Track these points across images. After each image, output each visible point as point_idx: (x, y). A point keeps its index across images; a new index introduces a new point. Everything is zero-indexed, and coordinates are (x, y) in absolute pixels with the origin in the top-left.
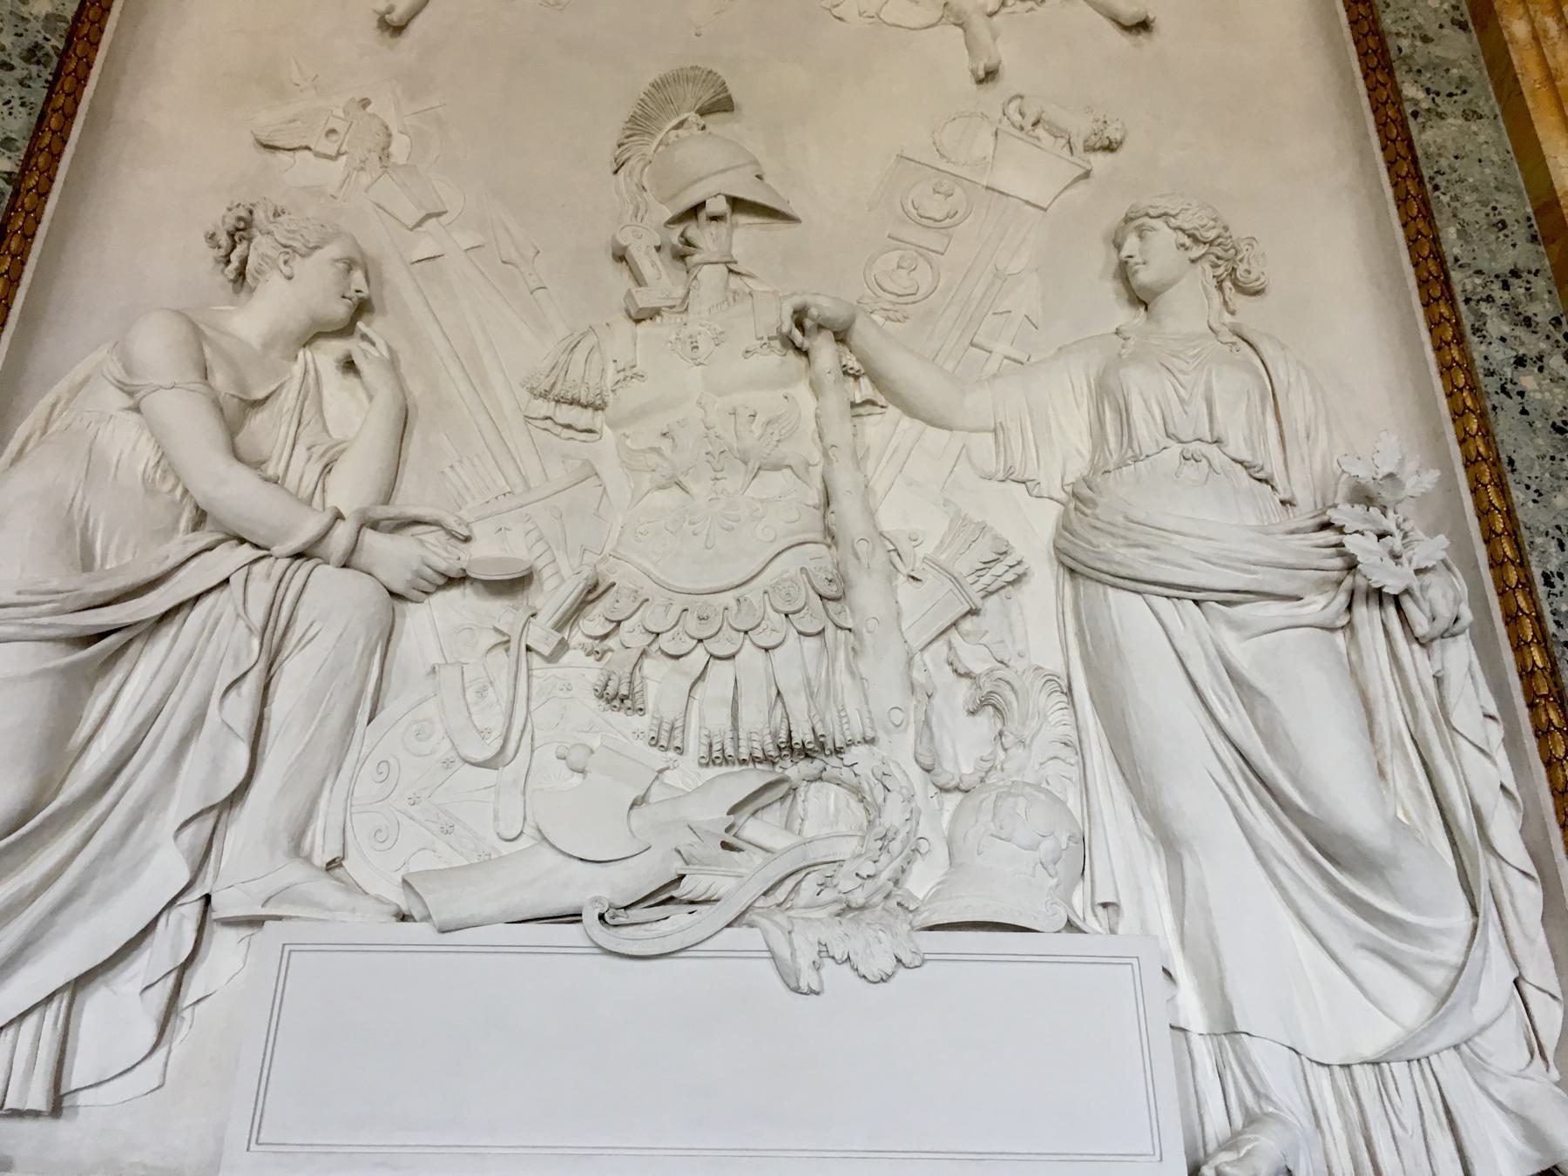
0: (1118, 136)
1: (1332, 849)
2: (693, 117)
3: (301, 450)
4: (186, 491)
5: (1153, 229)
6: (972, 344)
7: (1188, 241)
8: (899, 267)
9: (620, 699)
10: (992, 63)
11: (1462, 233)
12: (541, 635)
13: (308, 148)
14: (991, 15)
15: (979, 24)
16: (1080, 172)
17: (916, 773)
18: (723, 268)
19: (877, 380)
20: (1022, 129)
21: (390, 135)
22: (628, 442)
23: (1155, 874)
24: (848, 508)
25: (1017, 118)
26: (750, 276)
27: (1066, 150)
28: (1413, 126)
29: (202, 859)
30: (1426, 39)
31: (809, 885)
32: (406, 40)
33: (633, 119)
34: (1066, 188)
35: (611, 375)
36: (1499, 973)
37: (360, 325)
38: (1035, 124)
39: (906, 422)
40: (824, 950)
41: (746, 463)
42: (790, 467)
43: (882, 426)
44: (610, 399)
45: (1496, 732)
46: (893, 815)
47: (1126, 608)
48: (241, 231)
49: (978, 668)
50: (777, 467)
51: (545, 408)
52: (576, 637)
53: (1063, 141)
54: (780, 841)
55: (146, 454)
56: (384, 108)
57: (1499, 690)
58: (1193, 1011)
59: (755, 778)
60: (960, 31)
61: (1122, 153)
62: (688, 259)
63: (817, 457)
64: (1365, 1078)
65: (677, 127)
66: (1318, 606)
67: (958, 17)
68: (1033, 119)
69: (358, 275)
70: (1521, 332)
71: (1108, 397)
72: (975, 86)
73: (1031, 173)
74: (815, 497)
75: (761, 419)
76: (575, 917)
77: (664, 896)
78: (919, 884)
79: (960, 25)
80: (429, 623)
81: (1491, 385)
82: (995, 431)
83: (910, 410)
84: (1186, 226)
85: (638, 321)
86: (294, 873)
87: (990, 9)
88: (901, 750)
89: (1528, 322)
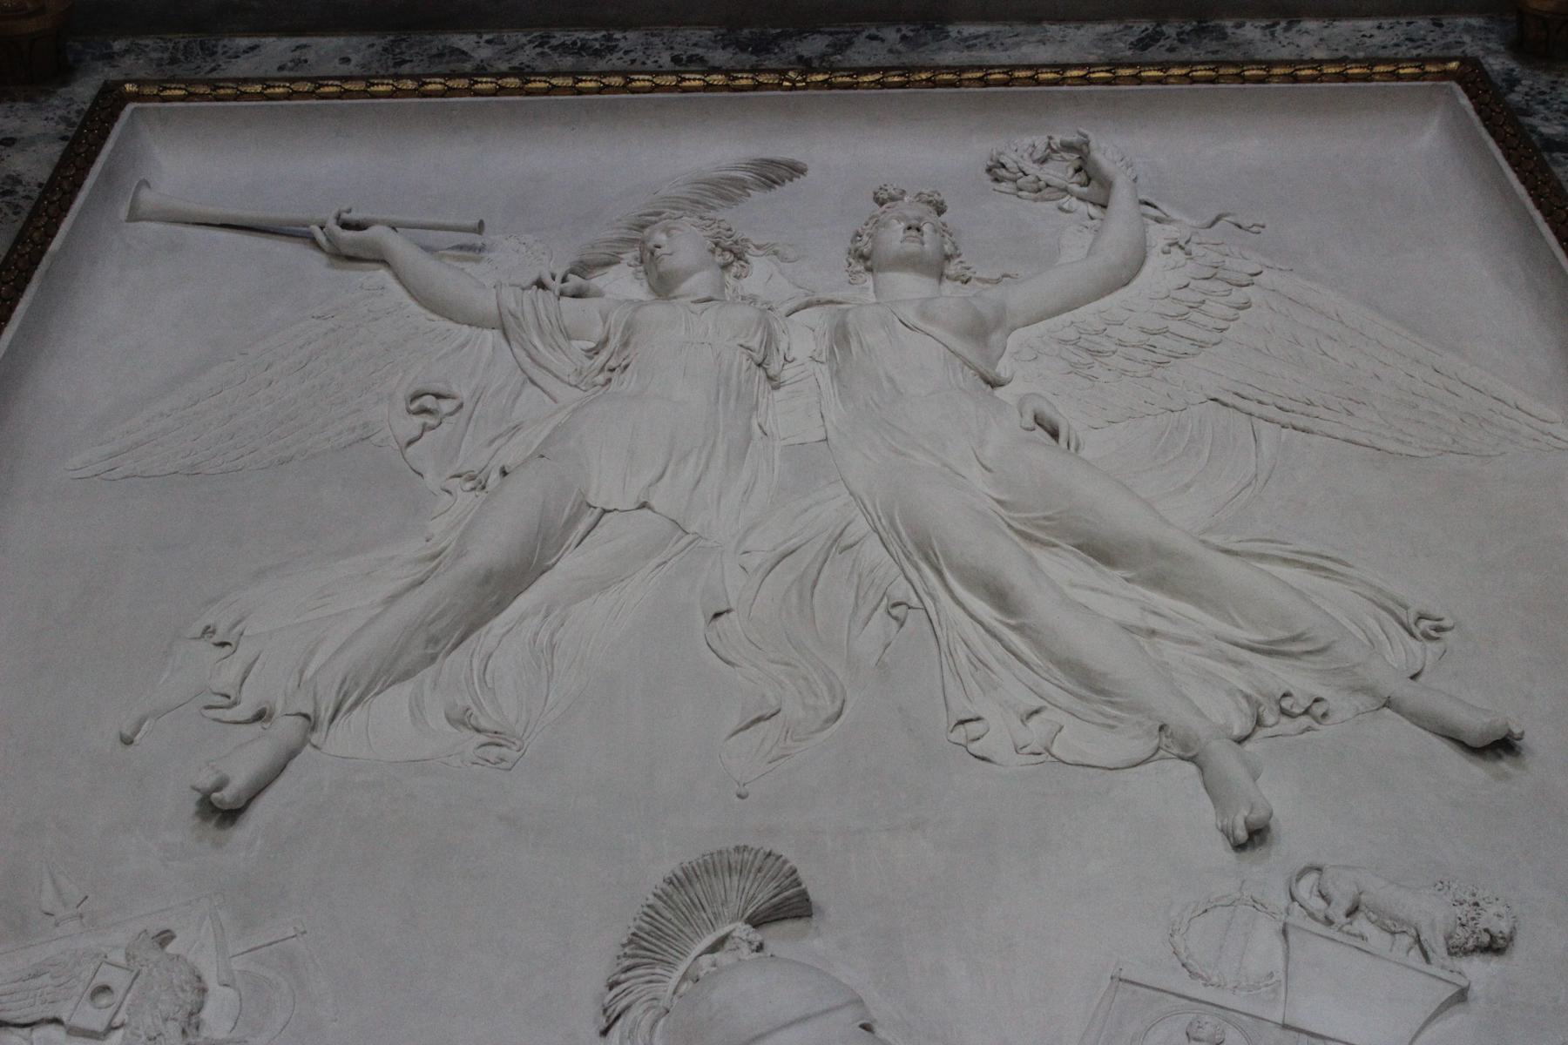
0: (1503, 926)
2: (741, 929)
10: (1258, 815)
13: (56, 1021)
14: (1241, 741)
15: (1226, 759)
16: (1451, 991)
20: (1329, 922)
21: (204, 991)
25: (1317, 904)
27: (1415, 953)
32: (242, 832)
33: (634, 939)
38: (1352, 912)
53: (1406, 940)
56: (198, 946)
60: (1191, 768)
65: (713, 949)
67: (1185, 746)
68: (1346, 905)
72: (1231, 856)
79: (1192, 760)
87: (1237, 731)
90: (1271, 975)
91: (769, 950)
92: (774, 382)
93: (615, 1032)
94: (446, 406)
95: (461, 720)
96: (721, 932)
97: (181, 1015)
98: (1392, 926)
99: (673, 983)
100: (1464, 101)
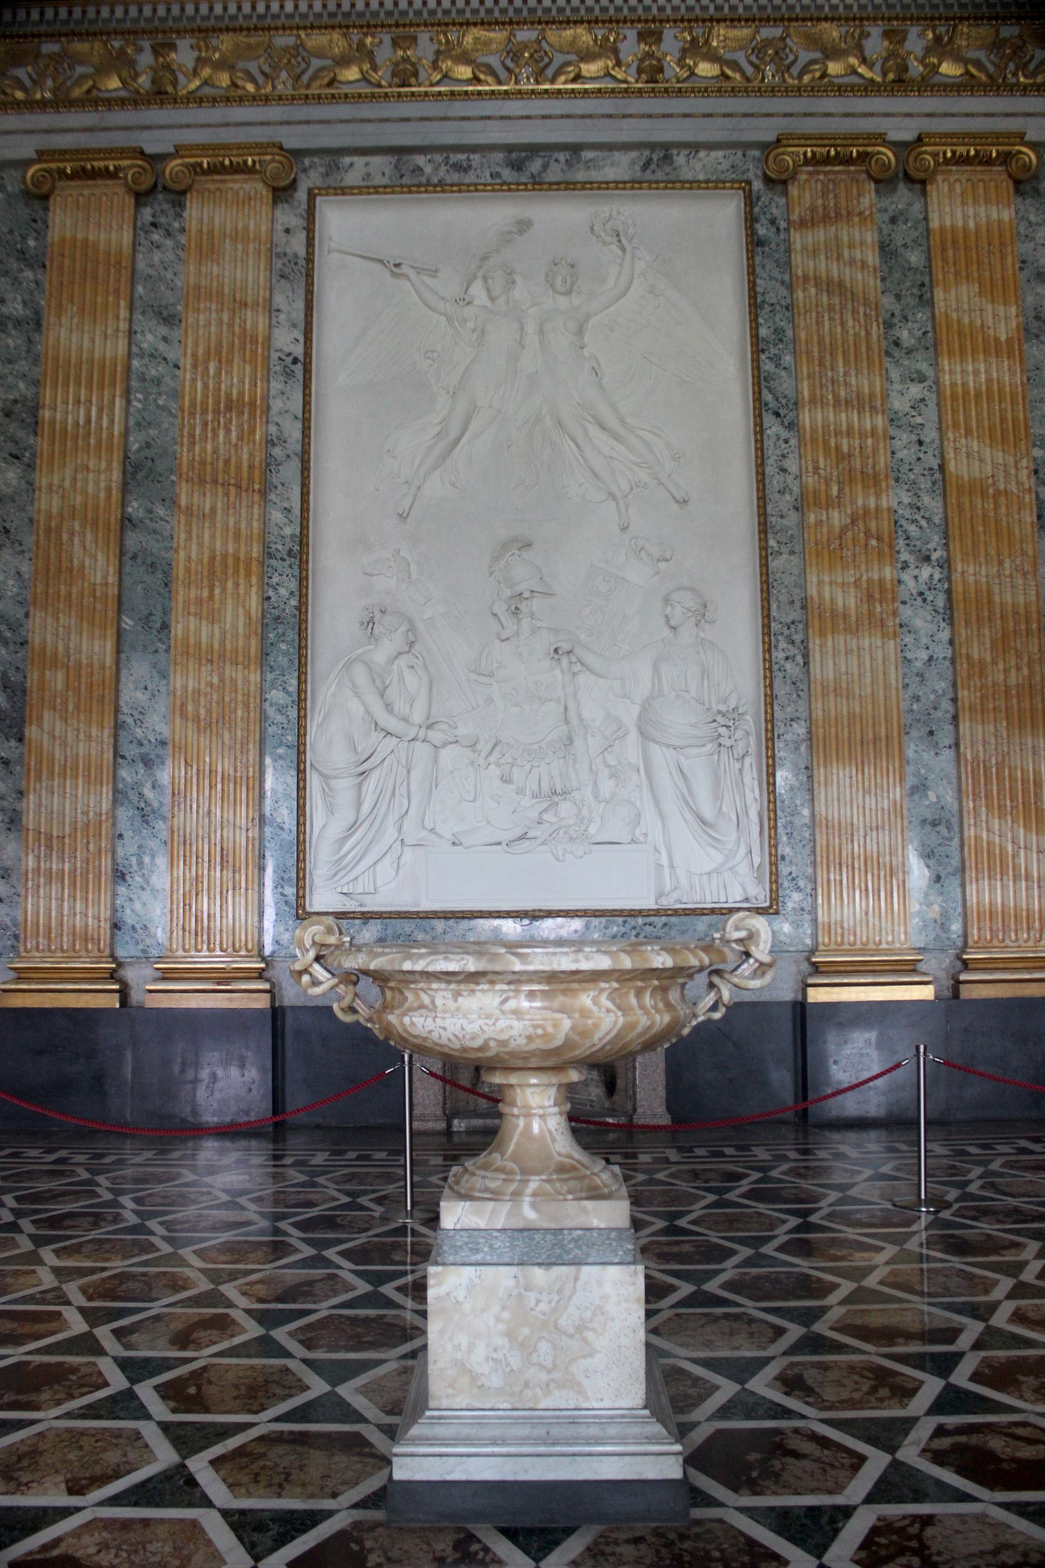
1: (703, 821)
9: (506, 780)
11: (778, 607)
12: (481, 761)
17: (591, 798)
19: (582, 664)
23: (659, 824)
24: (572, 715)
28: (770, 558)
29: (400, 830)
30: (782, 517)
31: (562, 832)
32: (409, 519)
35: (495, 665)
36: (743, 850)
39: (592, 677)
40: (565, 851)
43: (584, 679)
45: (756, 783)
46: (585, 812)
47: (655, 750)
48: (372, 621)
49: (612, 763)
51: (474, 676)
52: (492, 759)
54: (554, 820)
55: (362, 710)
57: (760, 771)
58: (664, 860)
59: (546, 805)
64: (706, 877)
66: (709, 747)
70: (790, 647)
71: (656, 669)
74: (562, 709)
76: (499, 843)
77: (523, 837)
78: (592, 829)
80: (447, 755)
81: (775, 667)
83: (593, 672)
86: (424, 834)
88: (588, 792)
89: (793, 642)
94: (435, 355)
95: (453, 485)
98: (649, 555)
100: (742, 205)
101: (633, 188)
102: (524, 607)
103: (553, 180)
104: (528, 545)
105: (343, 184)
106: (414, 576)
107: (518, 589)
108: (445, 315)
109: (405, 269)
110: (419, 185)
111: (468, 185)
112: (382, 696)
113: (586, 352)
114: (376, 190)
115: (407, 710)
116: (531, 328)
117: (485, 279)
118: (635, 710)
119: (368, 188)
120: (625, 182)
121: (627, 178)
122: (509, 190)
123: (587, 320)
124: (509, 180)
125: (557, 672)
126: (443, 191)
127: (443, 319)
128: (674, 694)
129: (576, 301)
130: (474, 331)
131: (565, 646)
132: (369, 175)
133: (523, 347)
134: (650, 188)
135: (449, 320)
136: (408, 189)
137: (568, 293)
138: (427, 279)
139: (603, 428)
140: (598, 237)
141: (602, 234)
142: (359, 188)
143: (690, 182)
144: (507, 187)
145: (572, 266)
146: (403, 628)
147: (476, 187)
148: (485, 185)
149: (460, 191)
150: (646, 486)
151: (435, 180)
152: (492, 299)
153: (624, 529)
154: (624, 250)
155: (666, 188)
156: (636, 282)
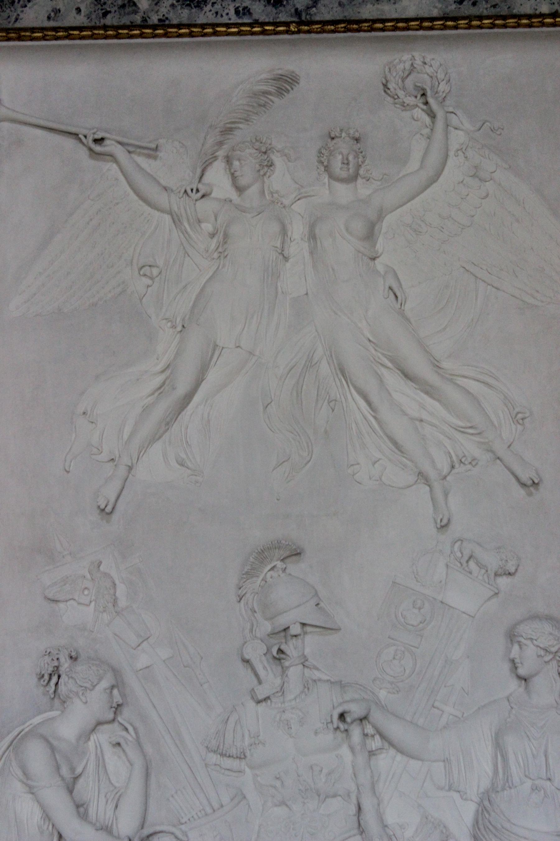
2: (279, 564)
3: (102, 796)
4: (53, 825)
5: (526, 645)
6: (433, 706)
7: (542, 653)
8: (394, 658)
13: (75, 600)
16: (492, 593)
18: (301, 666)
22: (259, 779)
24: (369, 817)
26: (317, 669)
32: (115, 517)
34: (485, 602)
35: (247, 741)
37: (119, 719)
39: (399, 757)
41: (319, 796)
42: (340, 795)
43: (386, 761)
44: (248, 754)
48: (56, 673)
50: (335, 796)
51: (214, 758)
55: (37, 814)
60: (428, 488)
61: (518, 574)
62: (282, 661)
63: (353, 788)
69: (115, 692)
71: (498, 745)
72: (435, 530)
73: (465, 596)
74: (353, 809)
75: (325, 771)
79: (429, 486)
82: (444, 761)
84: (541, 646)
85: (259, 702)
90: (441, 582)
91: (287, 571)
92: (286, 259)
93: (242, 601)
94: (155, 271)
95: (182, 464)
96: (272, 565)
97: (112, 600)
98: (480, 565)
99: (259, 582)
101: (445, 27)
102: (290, 648)
103: (328, 17)
104: (297, 554)
105: (18, 25)
106: (123, 602)
107: (282, 621)
108: (170, 213)
109: (110, 147)
110: (131, 26)
111: (203, 26)
112: (71, 791)
113: (379, 265)
114: (69, 33)
115: (110, 813)
116: (298, 230)
117: (228, 160)
118: (469, 811)
119: (55, 29)
120: (432, 19)
121: (435, 13)
122: (264, 32)
123: (381, 217)
124: (263, 18)
125: (345, 751)
126: (166, 35)
127: (167, 218)
128: (528, 784)
129: (363, 189)
130: (212, 235)
131: (356, 710)
132: (57, 11)
133: (286, 259)
134: (470, 27)
135: (176, 220)
136: (116, 32)
137: (353, 178)
138: (140, 160)
139: (407, 376)
140: (395, 97)
141: (401, 93)
142: (42, 29)
143: (529, 17)
144: (261, 28)
145: (357, 140)
146: (105, 684)
147: (213, 29)
148: (228, 25)
149: (191, 35)
150: (474, 462)
151: (154, 19)
152: (240, 190)
153: (443, 527)
154: (433, 116)
155: (493, 26)
156: (451, 162)
